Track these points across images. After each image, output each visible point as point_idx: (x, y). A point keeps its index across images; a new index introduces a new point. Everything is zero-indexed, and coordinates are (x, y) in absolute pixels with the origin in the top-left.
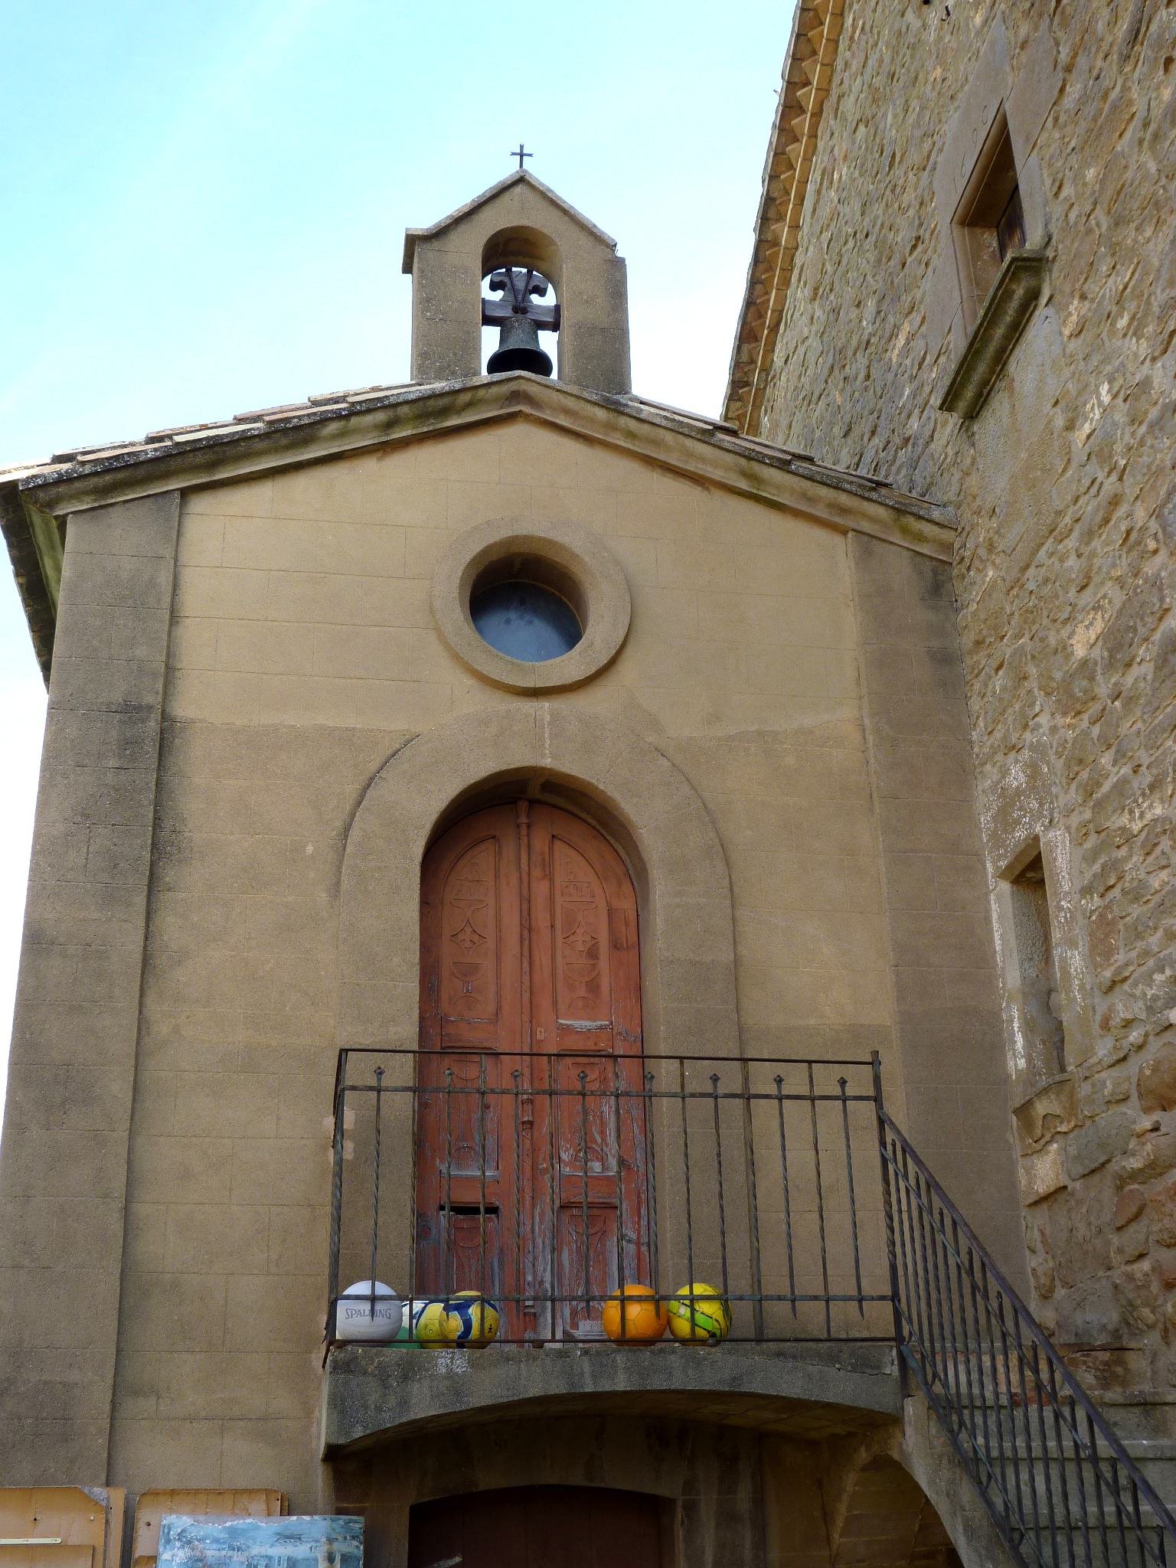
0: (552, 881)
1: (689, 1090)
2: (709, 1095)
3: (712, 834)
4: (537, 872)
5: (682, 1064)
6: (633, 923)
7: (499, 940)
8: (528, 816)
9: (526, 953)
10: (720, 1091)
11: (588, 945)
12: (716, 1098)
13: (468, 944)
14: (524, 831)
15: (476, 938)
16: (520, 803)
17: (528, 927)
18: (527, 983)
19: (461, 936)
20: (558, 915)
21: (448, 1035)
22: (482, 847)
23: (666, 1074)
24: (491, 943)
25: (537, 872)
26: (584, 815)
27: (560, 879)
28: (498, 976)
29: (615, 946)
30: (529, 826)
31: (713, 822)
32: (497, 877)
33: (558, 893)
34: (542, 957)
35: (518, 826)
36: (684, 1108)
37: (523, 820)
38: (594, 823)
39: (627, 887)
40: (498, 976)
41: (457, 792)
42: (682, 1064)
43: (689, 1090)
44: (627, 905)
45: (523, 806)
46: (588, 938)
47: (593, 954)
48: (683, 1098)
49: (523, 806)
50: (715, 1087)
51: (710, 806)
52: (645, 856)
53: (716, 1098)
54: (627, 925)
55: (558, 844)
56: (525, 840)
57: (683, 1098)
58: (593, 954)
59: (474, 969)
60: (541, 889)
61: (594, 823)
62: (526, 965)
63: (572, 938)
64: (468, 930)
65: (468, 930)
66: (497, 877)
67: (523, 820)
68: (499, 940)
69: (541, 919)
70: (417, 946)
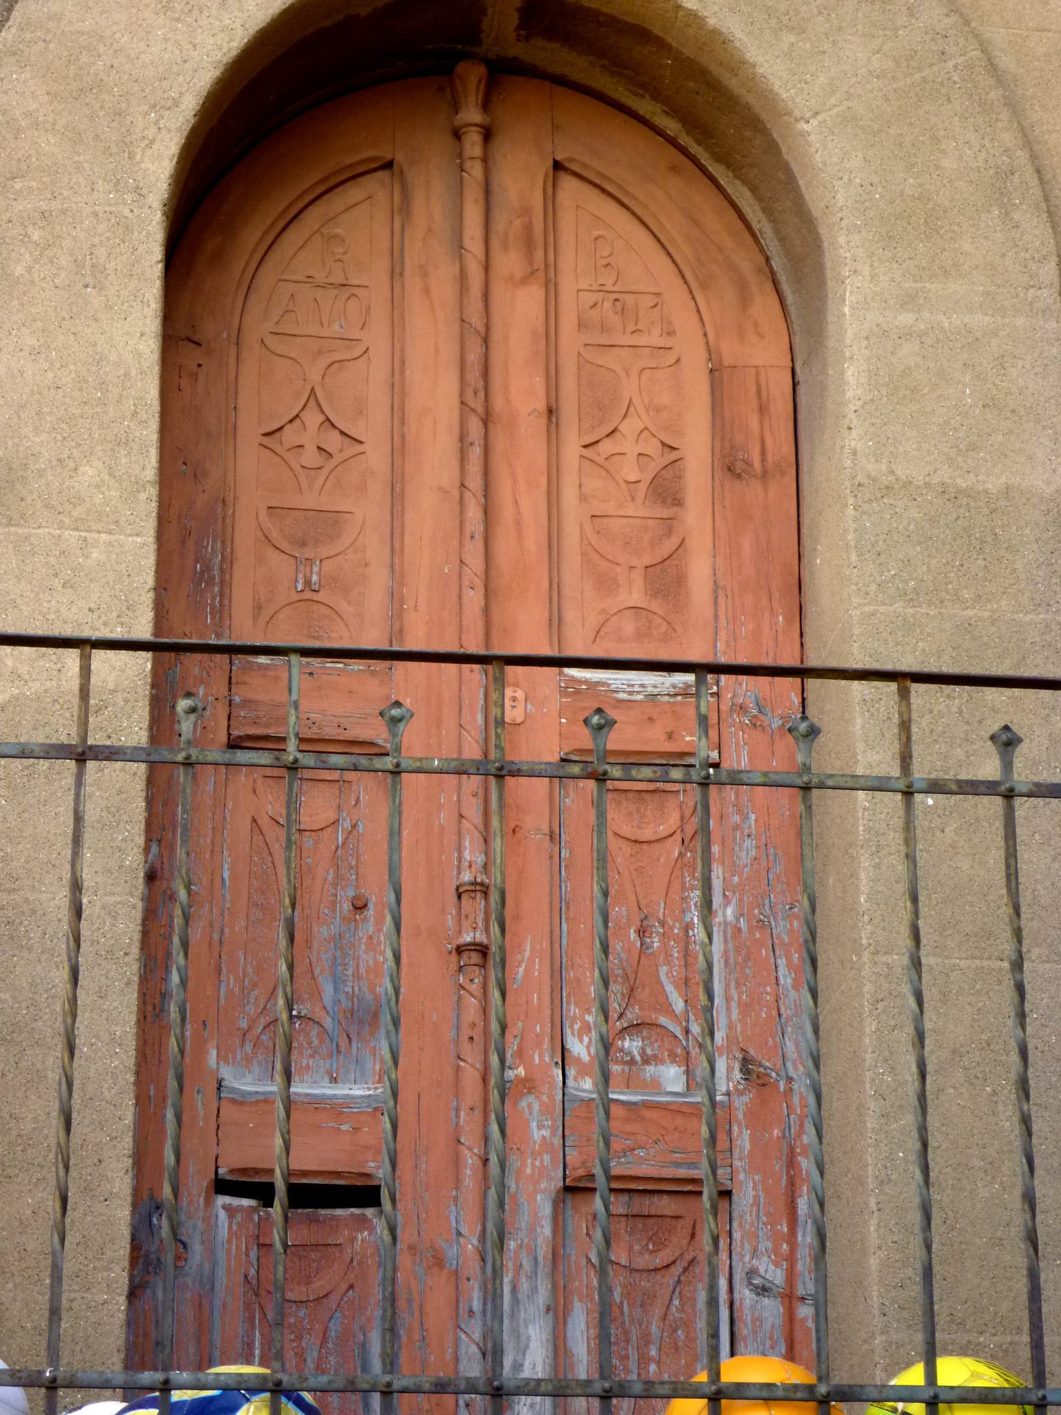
0: (551, 286)
1: (921, 771)
2: (989, 788)
3: (1008, 138)
4: (509, 262)
5: (904, 694)
6: (781, 406)
7: (399, 448)
8: (486, 105)
9: (475, 482)
10: (1023, 775)
11: (652, 468)
12: (1009, 795)
13: (310, 457)
14: (473, 144)
15: (333, 441)
16: (461, 68)
17: (481, 412)
18: (475, 561)
19: (290, 436)
20: (569, 385)
21: (246, 703)
22: (354, 192)
23: (859, 727)
24: (376, 457)
25: (509, 262)
26: (645, 106)
27: (575, 282)
28: (396, 549)
29: (731, 467)
30: (488, 135)
31: (1014, 106)
32: (396, 273)
33: (568, 321)
34: (522, 501)
35: (457, 134)
36: (909, 827)
37: (472, 114)
38: (671, 126)
39: (764, 306)
40: (396, 549)
41: (268, 19)
42: (904, 694)
43: (921, 771)
44: (765, 354)
45: (472, 76)
46: (653, 448)
47: (666, 490)
48: (908, 794)
49: (472, 76)
50: (1007, 766)
51: (1005, 61)
52: (814, 198)
53: (1009, 795)
54: (763, 409)
55: (569, 188)
56: (476, 171)
57: (908, 794)
58: (666, 490)
59: (326, 525)
60: (520, 309)
61: (671, 126)
62: (474, 513)
63: (607, 447)
64: (313, 419)
65: (313, 419)
66: (396, 273)
67: (472, 114)
68: (399, 448)
69: (521, 391)
70: (150, 433)
